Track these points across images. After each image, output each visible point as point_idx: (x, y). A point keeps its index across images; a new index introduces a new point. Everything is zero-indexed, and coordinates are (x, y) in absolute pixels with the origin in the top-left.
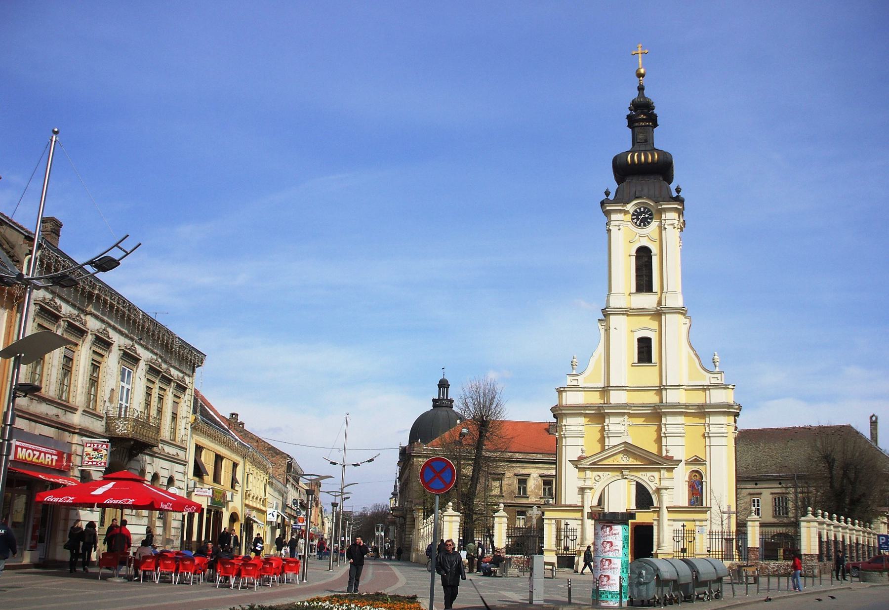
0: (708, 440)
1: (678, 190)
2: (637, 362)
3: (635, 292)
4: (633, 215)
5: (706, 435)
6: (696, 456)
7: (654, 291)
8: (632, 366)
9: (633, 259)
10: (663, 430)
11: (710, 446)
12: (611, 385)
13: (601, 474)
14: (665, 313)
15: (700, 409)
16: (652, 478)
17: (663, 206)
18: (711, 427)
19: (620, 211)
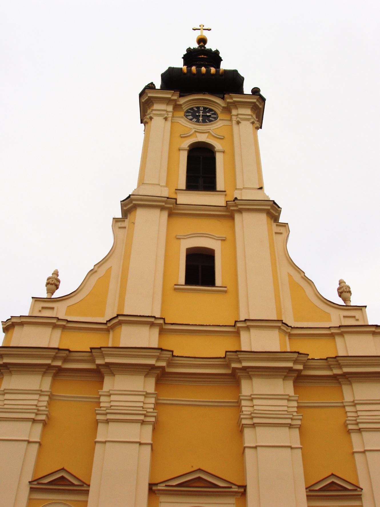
0: (355, 437)
1: (256, 91)
2: (183, 283)
3: (184, 187)
4: (187, 112)
5: (350, 427)
6: (332, 475)
7: (219, 188)
8: (175, 289)
9: (184, 156)
11: (364, 452)
14: (240, 211)
15: (330, 368)
17: (235, 99)
18: (359, 407)
19: (168, 101)
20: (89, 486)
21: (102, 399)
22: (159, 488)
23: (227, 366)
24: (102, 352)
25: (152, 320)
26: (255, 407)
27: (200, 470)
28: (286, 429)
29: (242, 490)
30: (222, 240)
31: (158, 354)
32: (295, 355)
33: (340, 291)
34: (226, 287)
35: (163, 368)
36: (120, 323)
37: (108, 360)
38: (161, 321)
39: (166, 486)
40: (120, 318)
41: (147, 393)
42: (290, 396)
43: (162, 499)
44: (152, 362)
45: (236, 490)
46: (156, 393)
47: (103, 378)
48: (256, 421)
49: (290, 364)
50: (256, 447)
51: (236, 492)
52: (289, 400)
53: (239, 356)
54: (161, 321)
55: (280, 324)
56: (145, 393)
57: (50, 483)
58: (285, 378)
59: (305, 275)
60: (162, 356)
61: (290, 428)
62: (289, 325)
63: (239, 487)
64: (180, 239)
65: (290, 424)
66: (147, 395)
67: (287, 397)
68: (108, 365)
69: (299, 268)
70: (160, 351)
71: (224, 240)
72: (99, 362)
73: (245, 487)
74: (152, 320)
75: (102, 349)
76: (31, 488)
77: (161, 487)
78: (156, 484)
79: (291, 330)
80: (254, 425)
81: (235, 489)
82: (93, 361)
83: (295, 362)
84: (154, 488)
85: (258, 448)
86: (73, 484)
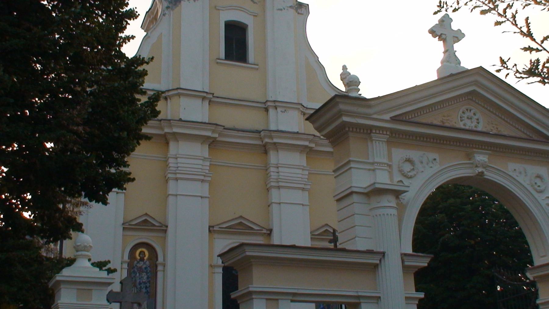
10: (274, 175)
12: (182, 87)
13: (414, 154)
16: (539, 182)
20: (167, 227)
21: (171, 160)
22: (215, 229)
23: (261, 139)
24: (171, 123)
25: (205, 95)
26: (280, 174)
27: (241, 217)
28: (300, 191)
29: (268, 232)
30: (254, 16)
31: (214, 128)
32: (311, 137)
33: (343, 77)
34: (258, 65)
35: (216, 138)
36: (179, 95)
37: (175, 130)
38: (211, 96)
39: (220, 228)
40: (180, 91)
41: (205, 158)
42: (304, 167)
43: (216, 236)
44: (209, 134)
45: (265, 232)
46: (210, 158)
47: (168, 143)
48: (281, 184)
49: (306, 143)
50: (280, 204)
51: (265, 233)
52: (303, 170)
53: (272, 134)
54: (211, 96)
55: (299, 107)
56: (203, 158)
57: (136, 225)
58: (301, 152)
59: (319, 59)
60: (216, 129)
61: (302, 190)
62: (305, 106)
63: (267, 230)
64: (219, 10)
65: (303, 188)
66: (205, 159)
67: (302, 167)
68: (174, 134)
69: (314, 53)
70: (215, 126)
71: (256, 16)
72: (167, 130)
73: (271, 230)
74: (205, 95)
75: (171, 121)
76: (124, 228)
77: (216, 228)
78: (213, 227)
79: (306, 110)
80: (279, 187)
81: (265, 231)
82: (162, 128)
83: (310, 141)
84: (211, 229)
85: (281, 204)
86: (154, 225)
